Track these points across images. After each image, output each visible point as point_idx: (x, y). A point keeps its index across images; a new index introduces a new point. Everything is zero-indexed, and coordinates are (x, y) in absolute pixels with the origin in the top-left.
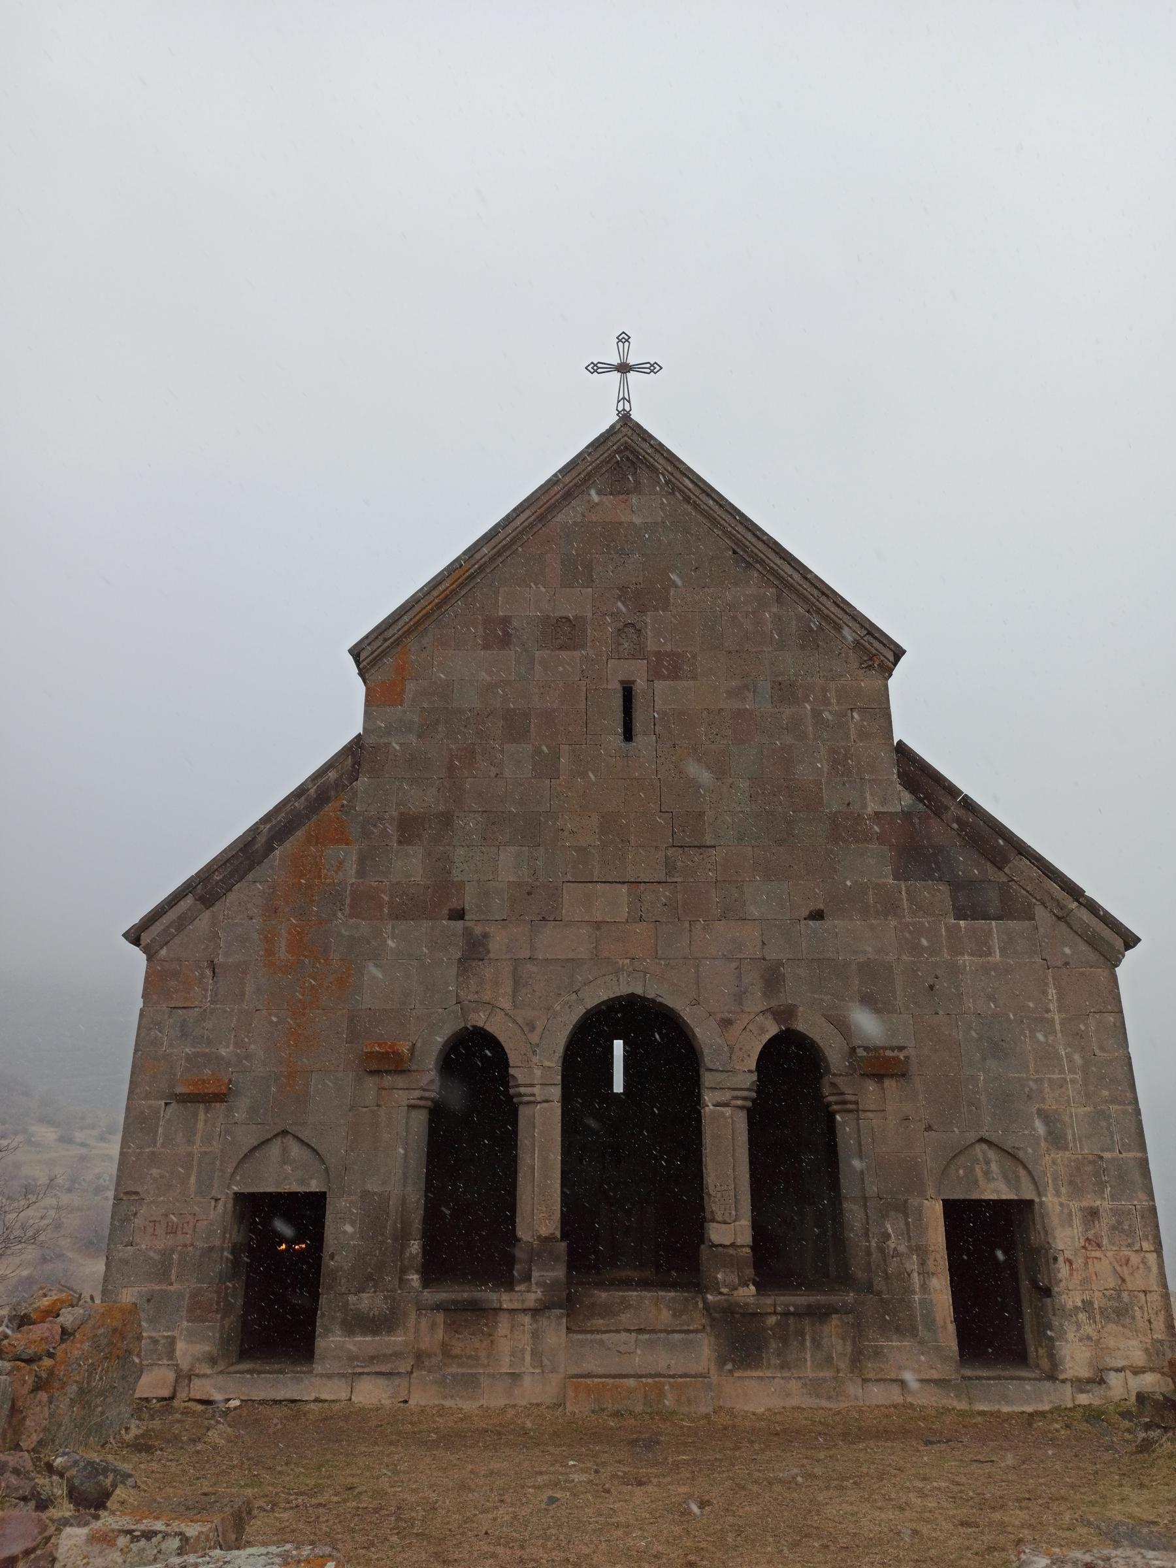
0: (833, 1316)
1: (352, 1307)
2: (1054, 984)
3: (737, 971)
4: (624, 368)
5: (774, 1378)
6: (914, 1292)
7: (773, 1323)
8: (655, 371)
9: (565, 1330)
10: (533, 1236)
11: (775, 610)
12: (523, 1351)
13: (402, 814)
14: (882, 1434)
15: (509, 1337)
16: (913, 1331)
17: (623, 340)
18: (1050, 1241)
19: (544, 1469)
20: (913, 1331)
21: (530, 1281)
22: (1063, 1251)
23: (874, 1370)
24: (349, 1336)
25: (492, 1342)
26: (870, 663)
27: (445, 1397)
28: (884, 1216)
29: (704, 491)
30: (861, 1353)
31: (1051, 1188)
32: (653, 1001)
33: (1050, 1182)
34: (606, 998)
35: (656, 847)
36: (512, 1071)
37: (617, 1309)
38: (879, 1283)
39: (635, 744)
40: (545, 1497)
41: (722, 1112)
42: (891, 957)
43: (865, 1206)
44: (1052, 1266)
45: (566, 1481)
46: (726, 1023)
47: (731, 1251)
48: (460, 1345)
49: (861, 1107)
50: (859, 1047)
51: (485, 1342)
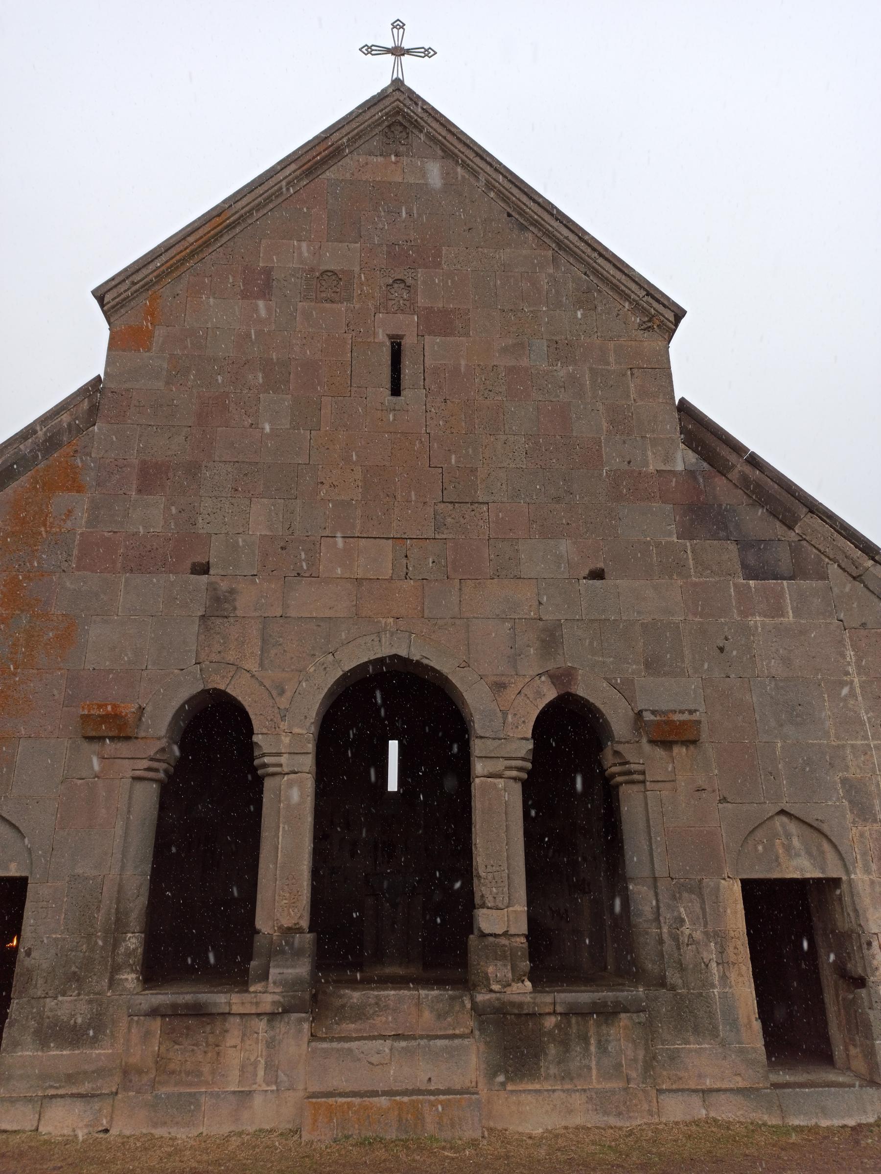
0: (623, 1015)
1: (49, 1014)
2: (852, 646)
4: (398, 52)
5: (554, 1091)
6: (713, 986)
7: (553, 1025)
8: (430, 55)
10: (274, 926)
11: (551, 271)
12: (255, 1064)
13: (144, 462)
15: (239, 1047)
18: (862, 924)
21: (267, 978)
22: (875, 934)
23: (670, 1079)
24: (42, 1050)
25: (218, 1054)
26: (650, 324)
27: (155, 1125)
29: (477, 154)
30: (654, 1058)
31: (860, 864)
32: (418, 663)
33: (858, 857)
35: (425, 503)
36: (255, 739)
37: (371, 1012)
38: (673, 977)
42: (677, 618)
43: (656, 887)
44: (865, 951)
46: (499, 687)
47: (504, 941)
49: (648, 778)
50: (646, 710)
51: (210, 1055)
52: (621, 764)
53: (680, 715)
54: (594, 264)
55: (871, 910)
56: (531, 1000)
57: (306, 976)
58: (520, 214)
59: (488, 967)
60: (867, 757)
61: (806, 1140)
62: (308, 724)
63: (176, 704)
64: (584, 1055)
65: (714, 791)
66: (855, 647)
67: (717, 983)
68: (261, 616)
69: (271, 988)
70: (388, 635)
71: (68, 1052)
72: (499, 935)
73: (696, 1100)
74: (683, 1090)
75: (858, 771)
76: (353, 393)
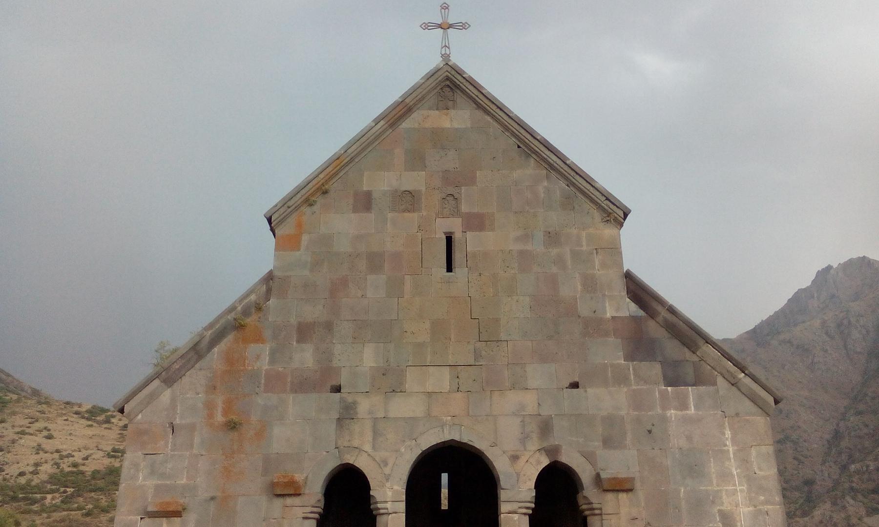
2: (729, 427)
3: (522, 423)
4: (445, 27)
17: (445, 8)
26: (608, 219)
36: (372, 493)
39: (454, 274)
42: (623, 413)
46: (515, 458)
58: (526, 146)
65: (642, 520)
70: (447, 427)
76: (423, 272)
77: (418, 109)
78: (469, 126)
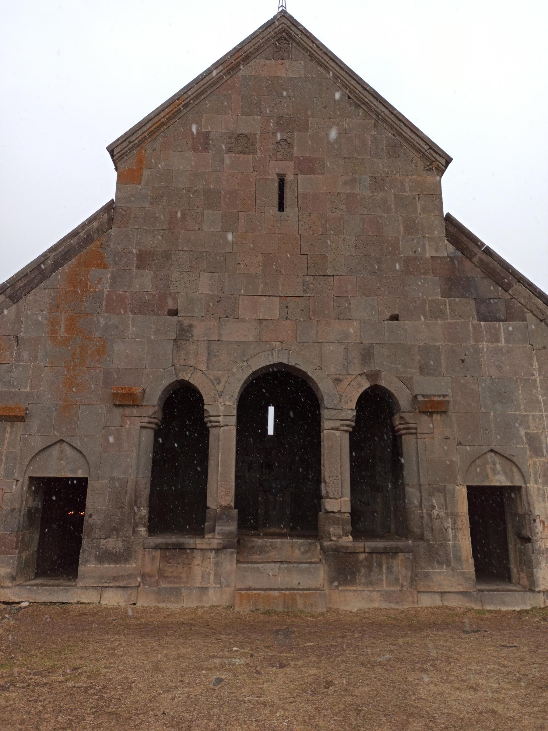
0: (400, 554)
2: (537, 359)
5: (363, 591)
6: (449, 540)
7: (363, 558)
9: (235, 561)
10: (217, 505)
12: (209, 574)
14: (434, 626)
15: (200, 565)
16: (448, 563)
19: (216, 654)
20: (448, 563)
22: (539, 515)
24: (100, 564)
26: (431, 167)
27: (159, 602)
28: (431, 494)
29: (331, 59)
30: (416, 576)
31: (532, 479)
33: (532, 475)
34: (265, 365)
36: (205, 407)
37: (268, 550)
38: (428, 535)
39: (285, 213)
40: (213, 678)
41: (335, 434)
42: (439, 344)
44: (532, 524)
45: (229, 664)
46: (338, 381)
47: (338, 515)
48: (170, 570)
49: (419, 431)
50: (419, 395)
51: (186, 569)
52: (404, 424)
53: (438, 398)
54: (399, 129)
55: (537, 503)
56: (353, 546)
57: (235, 531)
59: (330, 528)
60: (541, 421)
61: (494, 616)
62: (234, 400)
63: (162, 387)
64: (379, 573)
65: (455, 439)
66: (538, 360)
67: (451, 539)
68: (207, 340)
69: (217, 536)
70: (277, 352)
71: (113, 566)
72: (336, 512)
73: (437, 597)
74: (431, 592)
75: (535, 429)
77: (255, 58)
78: (303, 76)
